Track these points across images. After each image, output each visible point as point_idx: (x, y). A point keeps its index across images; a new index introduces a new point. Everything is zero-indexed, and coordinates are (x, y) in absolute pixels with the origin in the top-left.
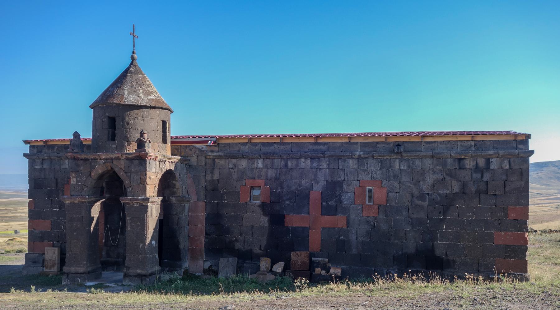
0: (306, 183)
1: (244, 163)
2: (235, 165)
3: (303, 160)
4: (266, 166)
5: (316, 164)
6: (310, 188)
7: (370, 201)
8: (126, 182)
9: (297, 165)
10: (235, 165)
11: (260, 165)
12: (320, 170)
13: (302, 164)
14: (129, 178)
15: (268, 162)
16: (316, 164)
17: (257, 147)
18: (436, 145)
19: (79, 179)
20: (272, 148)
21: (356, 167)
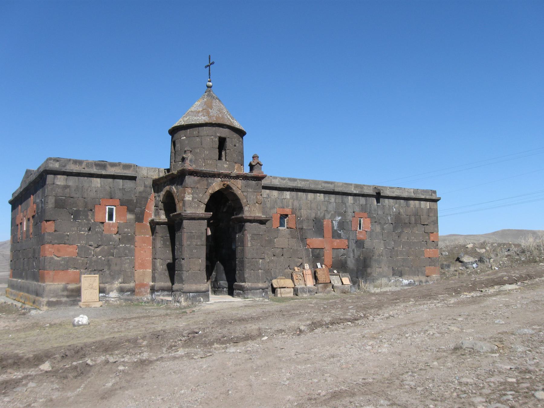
0: (321, 214)
1: (275, 193)
2: (268, 195)
3: (318, 194)
4: (292, 198)
5: (327, 198)
6: (324, 218)
7: (360, 228)
8: (243, 201)
9: (314, 198)
10: (268, 195)
11: (288, 197)
12: (330, 203)
13: (318, 197)
14: (246, 197)
15: (294, 193)
16: (327, 198)
17: (285, 181)
18: (394, 190)
19: (195, 195)
20: (296, 183)
21: (352, 202)
